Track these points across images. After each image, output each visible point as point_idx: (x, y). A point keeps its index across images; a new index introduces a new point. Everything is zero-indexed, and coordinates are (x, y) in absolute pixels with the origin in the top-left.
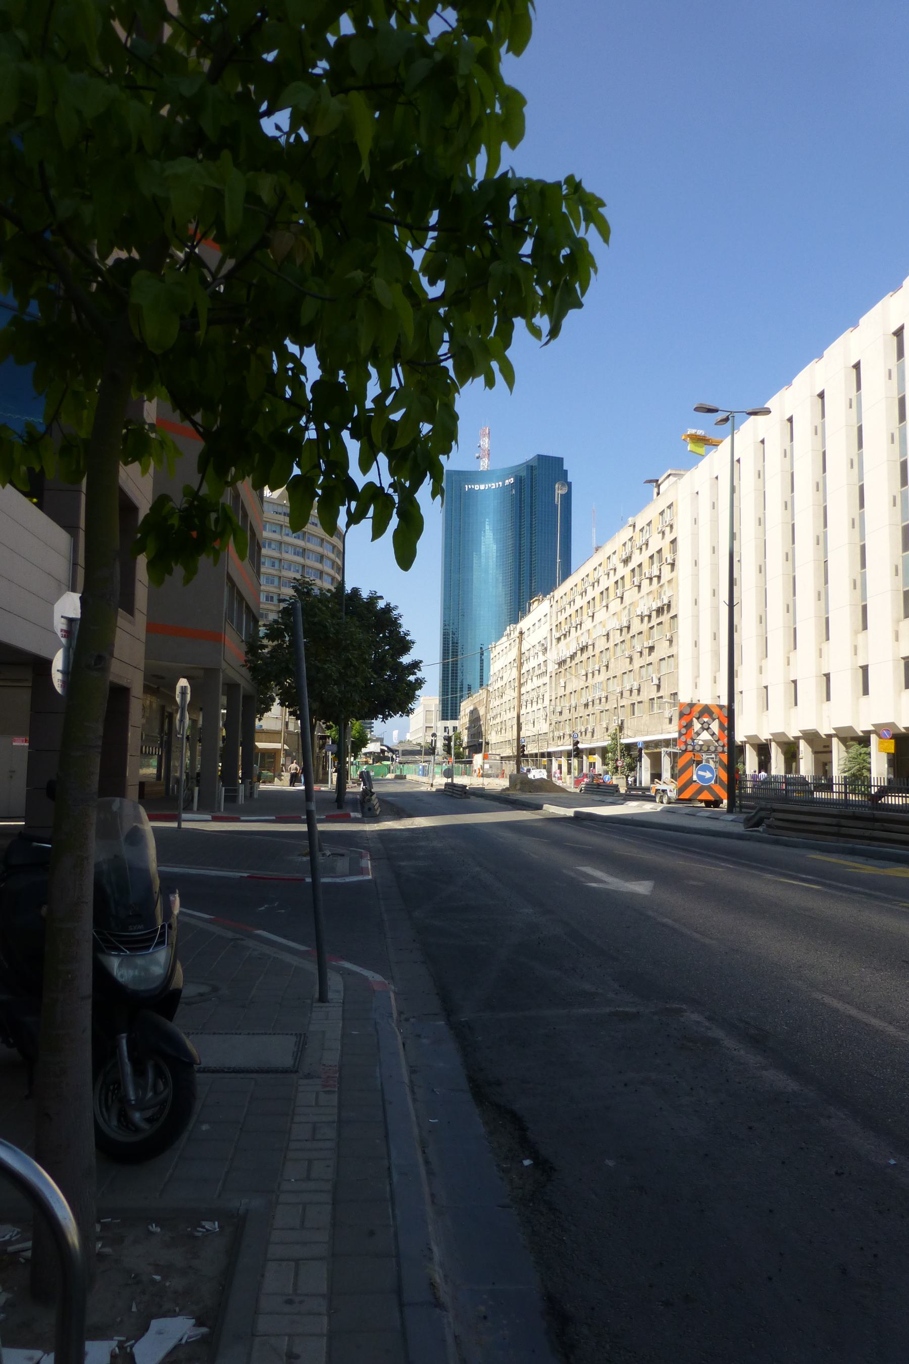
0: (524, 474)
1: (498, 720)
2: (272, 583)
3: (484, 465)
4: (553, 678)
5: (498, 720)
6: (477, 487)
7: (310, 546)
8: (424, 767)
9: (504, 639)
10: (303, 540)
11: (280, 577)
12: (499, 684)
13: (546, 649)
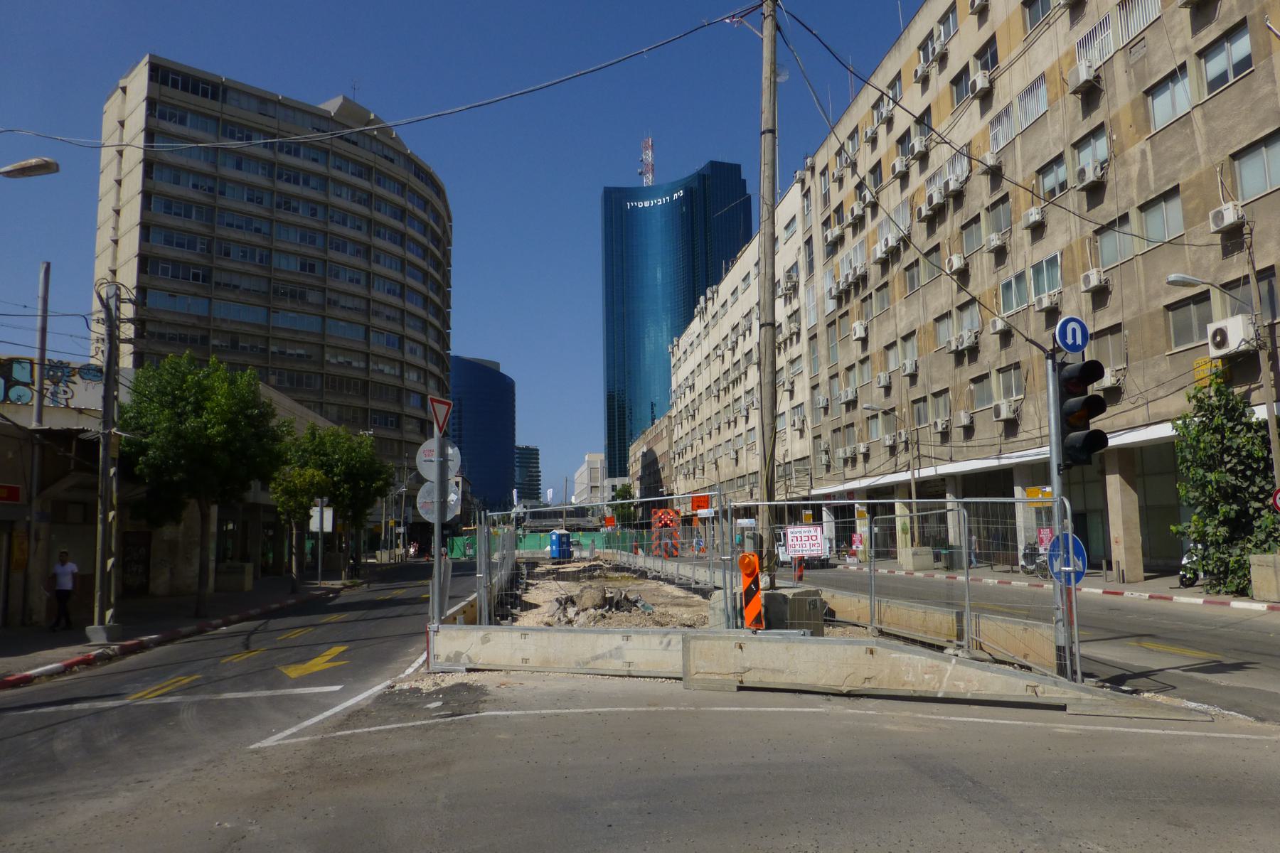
0: (695, 185)
1: (689, 456)
2: (313, 242)
3: (648, 180)
4: (822, 339)
5: (689, 456)
6: (640, 205)
7: (380, 191)
8: (560, 536)
9: (697, 319)
10: (369, 180)
11: (326, 234)
12: (689, 397)
13: (795, 288)
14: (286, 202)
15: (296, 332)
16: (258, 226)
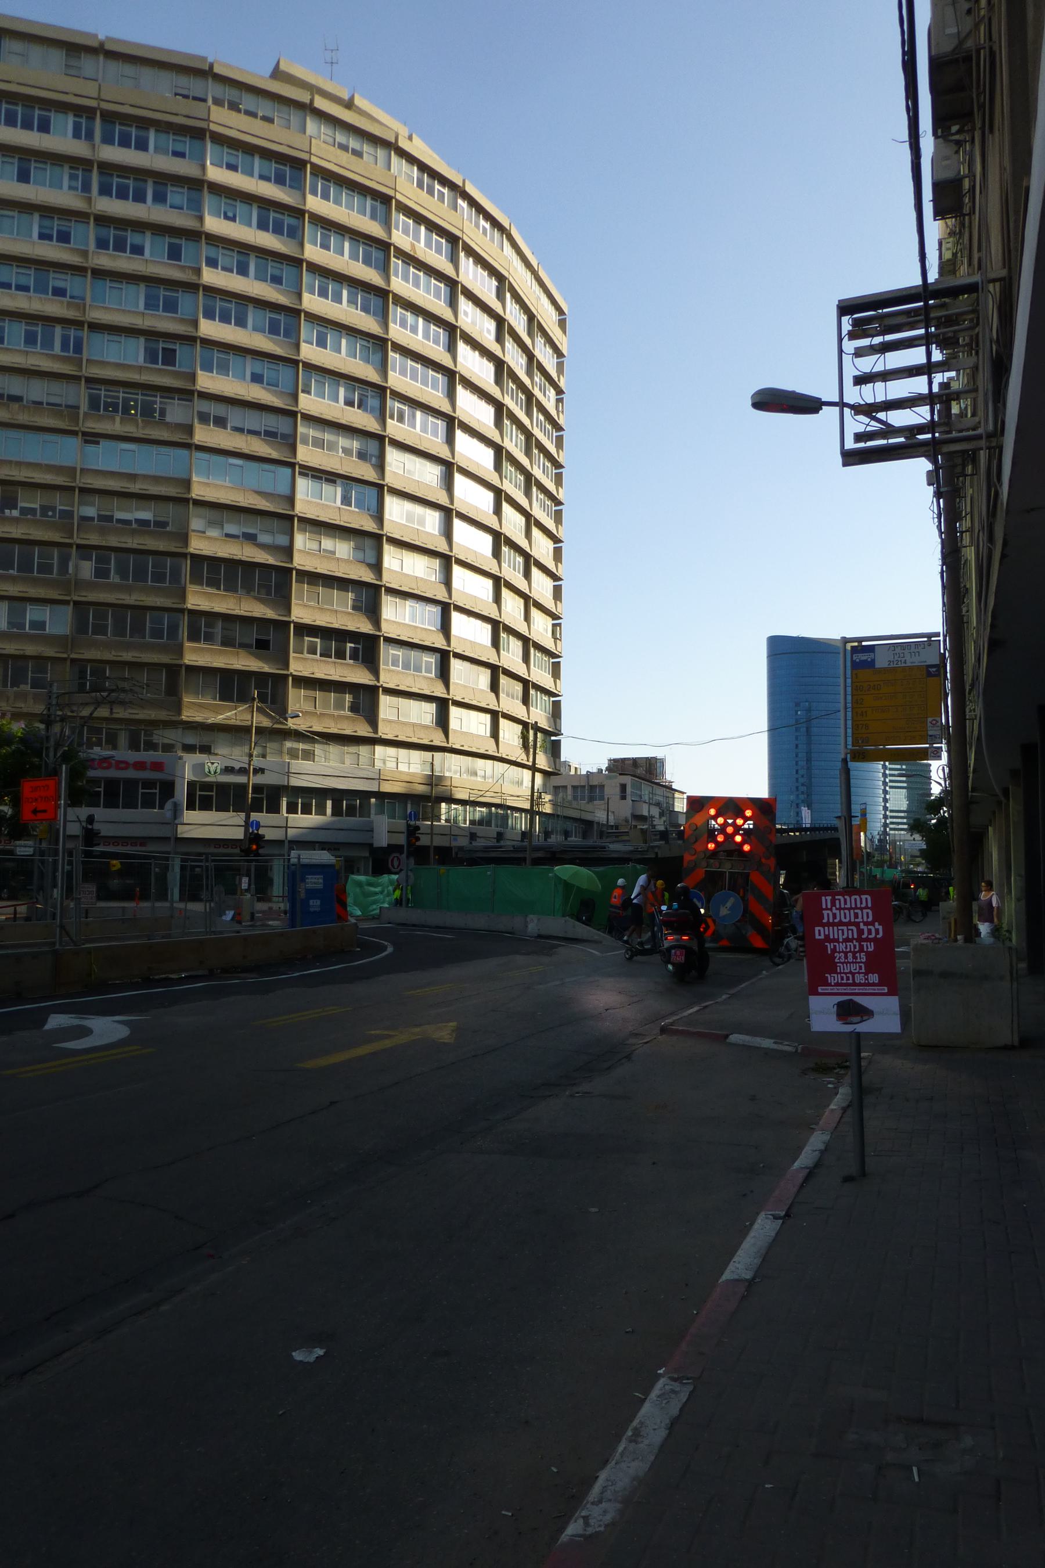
14: (117, 231)
15: (132, 477)
16: (60, 284)
